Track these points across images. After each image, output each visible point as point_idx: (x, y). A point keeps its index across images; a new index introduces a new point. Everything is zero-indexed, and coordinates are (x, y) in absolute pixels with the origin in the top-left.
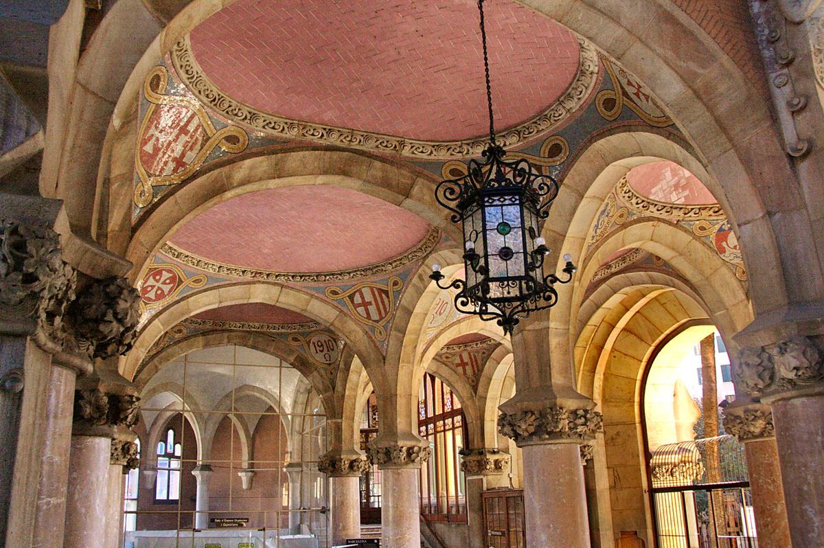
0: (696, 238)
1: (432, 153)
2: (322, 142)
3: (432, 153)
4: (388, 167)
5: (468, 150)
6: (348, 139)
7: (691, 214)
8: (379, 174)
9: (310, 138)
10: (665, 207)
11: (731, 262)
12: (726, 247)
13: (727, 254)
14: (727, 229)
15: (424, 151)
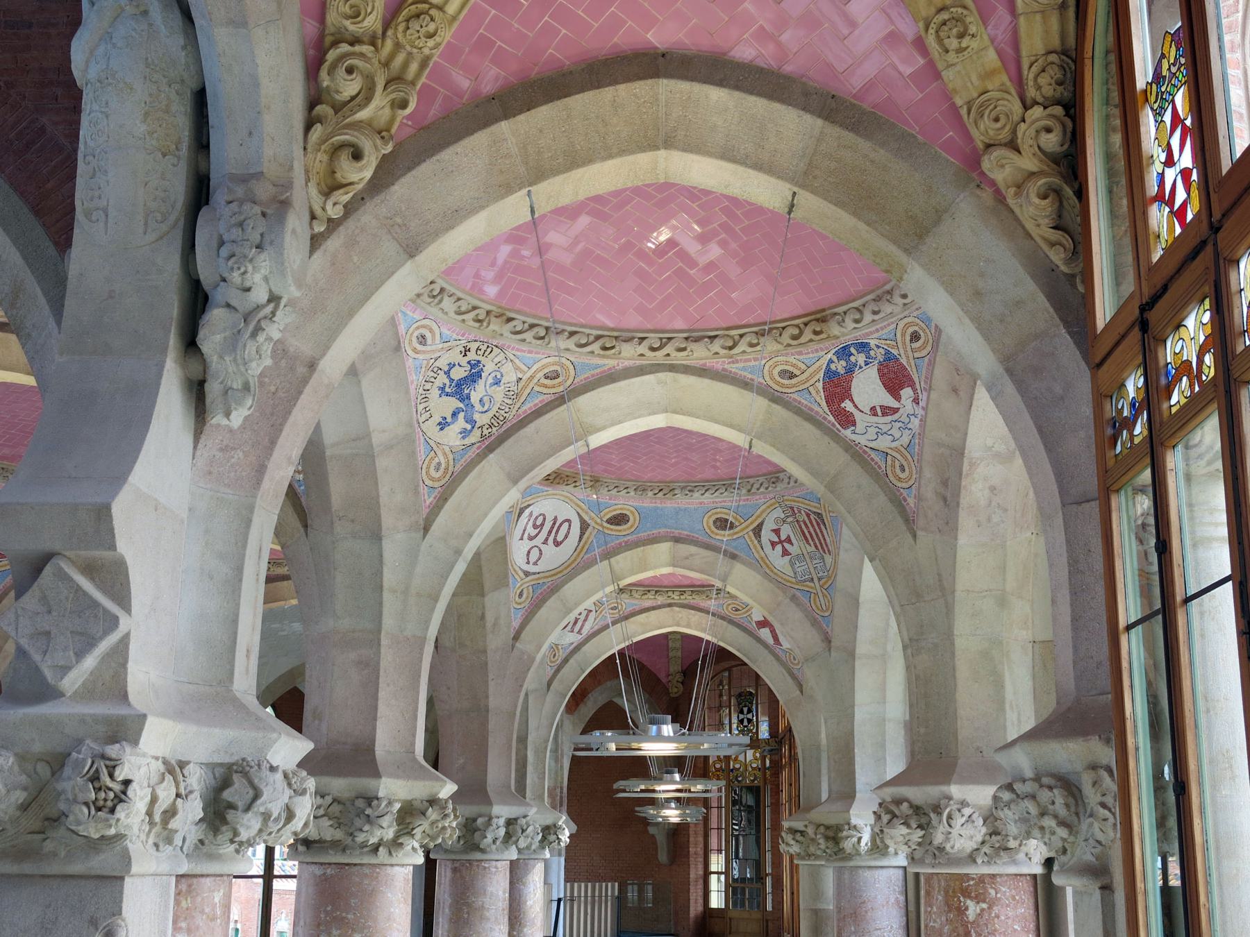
13: (860, 427)
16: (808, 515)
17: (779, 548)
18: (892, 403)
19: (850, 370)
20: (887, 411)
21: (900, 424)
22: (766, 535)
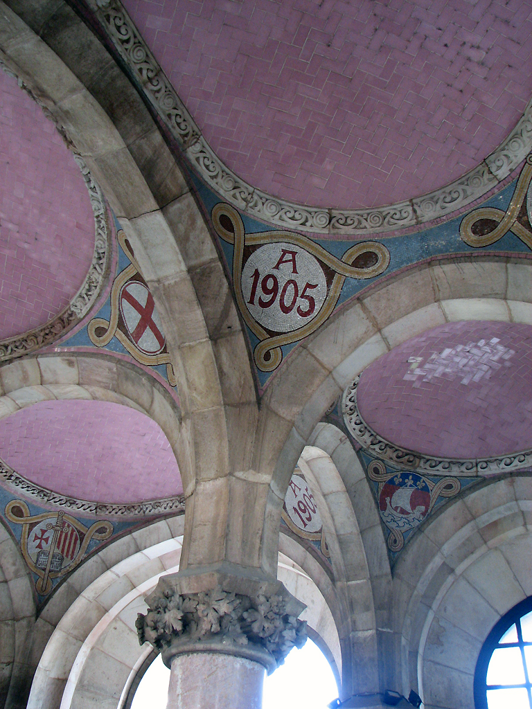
0: (369, 479)
1: (216, 177)
2: (119, 49)
3: (216, 177)
4: (166, 151)
5: (256, 205)
6: (151, 75)
7: (377, 447)
8: (149, 153)
9: (112, 29)
10: (361, 423)
11: (387, 524)
12: (388, 504)
14: (397, 483)
15: (211, 168)
16: (73, 531)
17: (38, 541)
18: (408, 508)
19: (402, 484)
20: (403, 512)
21: (406, 521)
22: (36, 529)
